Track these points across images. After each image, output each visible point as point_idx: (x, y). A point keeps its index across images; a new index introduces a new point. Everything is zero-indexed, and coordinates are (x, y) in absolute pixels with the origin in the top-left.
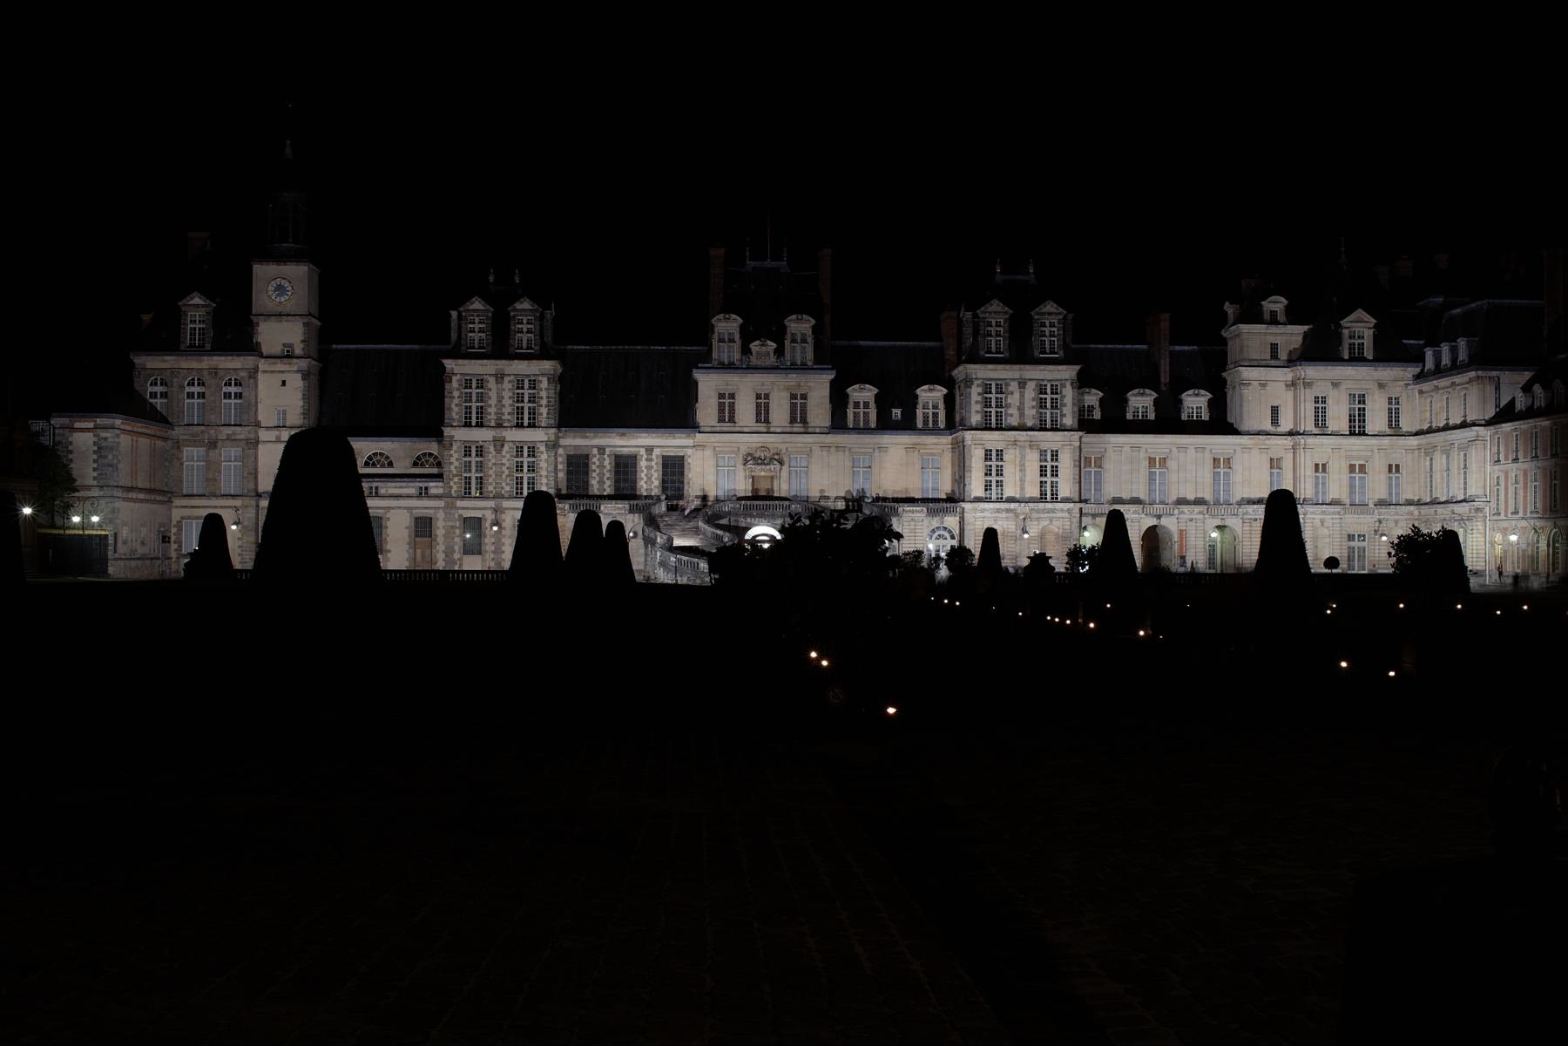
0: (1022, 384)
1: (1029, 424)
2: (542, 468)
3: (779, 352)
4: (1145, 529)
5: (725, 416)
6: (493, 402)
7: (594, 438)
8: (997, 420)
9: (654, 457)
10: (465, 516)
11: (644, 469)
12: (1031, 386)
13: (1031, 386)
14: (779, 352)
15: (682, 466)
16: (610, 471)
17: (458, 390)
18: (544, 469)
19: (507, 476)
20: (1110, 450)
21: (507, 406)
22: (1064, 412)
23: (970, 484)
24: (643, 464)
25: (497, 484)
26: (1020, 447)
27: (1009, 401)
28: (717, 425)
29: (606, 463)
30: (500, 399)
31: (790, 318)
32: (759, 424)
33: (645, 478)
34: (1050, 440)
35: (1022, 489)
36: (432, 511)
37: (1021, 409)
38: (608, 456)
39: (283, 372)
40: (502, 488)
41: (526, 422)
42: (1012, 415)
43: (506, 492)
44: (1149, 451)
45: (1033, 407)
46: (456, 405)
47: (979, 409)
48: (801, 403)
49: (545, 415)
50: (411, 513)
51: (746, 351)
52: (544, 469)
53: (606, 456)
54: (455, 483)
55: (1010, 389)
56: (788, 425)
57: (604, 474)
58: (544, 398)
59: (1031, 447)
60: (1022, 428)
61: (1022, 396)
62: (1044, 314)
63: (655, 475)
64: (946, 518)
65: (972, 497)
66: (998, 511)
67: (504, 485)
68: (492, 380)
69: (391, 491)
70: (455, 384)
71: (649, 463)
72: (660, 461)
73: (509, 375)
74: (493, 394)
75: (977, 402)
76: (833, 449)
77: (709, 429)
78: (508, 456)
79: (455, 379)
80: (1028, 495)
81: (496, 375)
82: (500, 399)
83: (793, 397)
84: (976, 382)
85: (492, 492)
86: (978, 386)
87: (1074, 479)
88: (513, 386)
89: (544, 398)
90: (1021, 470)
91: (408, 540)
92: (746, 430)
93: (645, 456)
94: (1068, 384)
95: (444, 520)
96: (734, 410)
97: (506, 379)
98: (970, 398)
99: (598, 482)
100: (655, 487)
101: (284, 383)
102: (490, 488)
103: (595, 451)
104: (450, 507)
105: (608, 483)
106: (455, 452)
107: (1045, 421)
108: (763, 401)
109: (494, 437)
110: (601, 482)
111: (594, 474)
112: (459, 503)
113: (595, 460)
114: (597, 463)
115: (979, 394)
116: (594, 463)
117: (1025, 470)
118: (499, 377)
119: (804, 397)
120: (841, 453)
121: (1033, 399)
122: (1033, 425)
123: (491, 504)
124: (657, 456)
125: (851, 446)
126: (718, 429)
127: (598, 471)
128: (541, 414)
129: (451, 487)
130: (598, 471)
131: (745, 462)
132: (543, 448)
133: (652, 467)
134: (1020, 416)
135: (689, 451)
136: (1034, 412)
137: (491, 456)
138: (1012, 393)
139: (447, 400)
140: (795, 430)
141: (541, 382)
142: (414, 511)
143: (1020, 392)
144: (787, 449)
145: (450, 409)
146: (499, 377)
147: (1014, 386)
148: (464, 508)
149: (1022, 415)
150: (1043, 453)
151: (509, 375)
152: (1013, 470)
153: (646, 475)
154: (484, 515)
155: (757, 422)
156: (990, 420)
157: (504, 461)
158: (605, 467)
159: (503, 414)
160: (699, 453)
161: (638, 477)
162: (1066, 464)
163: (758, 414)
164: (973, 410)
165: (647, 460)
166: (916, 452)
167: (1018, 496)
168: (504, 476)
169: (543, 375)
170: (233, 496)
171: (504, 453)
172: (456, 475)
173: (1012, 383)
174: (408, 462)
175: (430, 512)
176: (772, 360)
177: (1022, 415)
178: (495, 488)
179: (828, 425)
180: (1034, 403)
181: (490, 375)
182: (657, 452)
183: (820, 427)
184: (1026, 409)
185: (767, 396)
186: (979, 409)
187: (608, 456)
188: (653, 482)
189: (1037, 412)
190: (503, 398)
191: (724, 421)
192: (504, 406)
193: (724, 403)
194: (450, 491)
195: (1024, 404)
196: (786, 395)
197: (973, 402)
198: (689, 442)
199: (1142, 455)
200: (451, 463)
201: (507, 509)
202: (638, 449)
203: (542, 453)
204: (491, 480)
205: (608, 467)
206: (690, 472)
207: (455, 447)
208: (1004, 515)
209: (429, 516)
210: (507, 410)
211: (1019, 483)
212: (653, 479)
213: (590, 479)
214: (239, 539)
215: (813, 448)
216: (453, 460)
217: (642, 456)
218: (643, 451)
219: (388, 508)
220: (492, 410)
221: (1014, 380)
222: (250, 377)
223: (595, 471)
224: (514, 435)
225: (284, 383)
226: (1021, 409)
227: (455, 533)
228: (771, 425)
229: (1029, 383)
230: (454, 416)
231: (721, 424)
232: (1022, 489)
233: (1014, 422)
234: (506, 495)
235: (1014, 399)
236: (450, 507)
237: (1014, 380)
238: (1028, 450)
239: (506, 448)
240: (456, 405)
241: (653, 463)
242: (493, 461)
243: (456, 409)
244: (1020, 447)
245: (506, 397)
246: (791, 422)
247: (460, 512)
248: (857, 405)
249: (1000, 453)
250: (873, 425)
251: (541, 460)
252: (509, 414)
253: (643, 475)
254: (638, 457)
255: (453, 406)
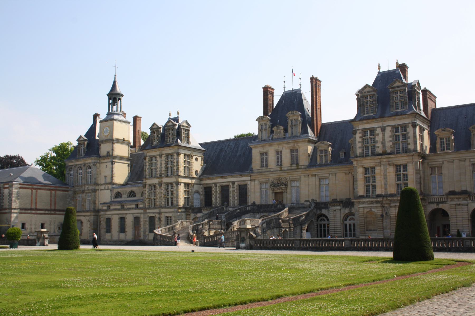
0: (383, 129)
1: (389, 151)
2: (174, 194)
3: (286, 131)
4: (472, 210)
5: (264, 164)
6: (159, 166)
7: (213, 179)
8: (372, 151)
9: (235, 186)
10: (150, 216)
11: (231, 192)
12: (388, 130)
13: (388, 130)
14: (286, 131)
15: (246, 189)
16: (219, 194)
17: (148, 162)
18: (175, 194)
19: (163, 198)
20: (445, 163)
21: (163, 167)
22: (409, 142)
23: (357, 188)
24: (231, 189)
25: (160, 201)
26: (383, 165)
27: (377, 139)
28: (260, 169)
29: (218, 190)
30: (161, 164)
31: (289, 113)
32: (277, 167)
33: (232, 196)
34: (401, 159)
35: (386, 189)
36: (139, 215)
37: (383, 143)
38: (218, 187)
39: (106, 162)
40: (161, 203)
41: (170, 174)
42: (378, 147)
43: (163, 205)
44: (472, 160)
45: (390, 141)
46: (148, 169)
47: (361, 146)
48: (296, 154)
49: (176, 170)
50: (133, 216)
51: (272, 132)
52: (175, 194)
53: (217, 187)
54: (147, 202)
55: (377, 132)
56: (290, 166)
57: (217, 195)
58: (176, 162)
59: (389, 164)
60: (384, 153)
61: (384, 135)
62: (394, 88)
63: (236, 194)
64: (352, 209)
65: (358, 195)
66: (372, 202)
67: (162, 202)
68: (158, 157)
69: (128, 207)
70: (147, 160)
71: (233, 189)
72: (238, 187)
73: (164, 154)
74: (159, 163)
75: (359, 142)
76: (310, 176)
77: (256, 171)
78: (163, 189)
79: (147, 158)
80: (389, 193)
81: (159, 155)
82: (161, 164)
83: (292, 151)
84: (358, 132)
85: (158, 205)
86: (360, 133)
87: (416, 181)
88: (165, 158)
89: (176, 162)
90: (384, 178)
91: (132, 227)
92: (272, 170)
93: (232, 186)
94: (410, 125)
95: (143, 218)
96: (267, 161)
97: (163, 156)
98: (356, 140)
99: (215, 199)
100: (236, 200)
101: (107, 165)
102: (158, 203)
103: (213, 185)
104: (145, 213)
105: (218, 199)
106: (147, 189)
107: (399, 148)
108: (279, 155)
109: (159, 181)
110: (216, 199)
111: (213, 196)
112: (148, 211)
113: (213, 189)
114: (214, 191)
115: (360, 137)
116: (213, 191)
117: (387, 178)
118: (161, 156)
119: (297, 150)
120: (314, 178)
121: (390, 137)
122: (391, 151)
123: (157, 211)
124: (236, 186)
125: (319, 173)
126: (260, 170)
127: (214, 194)
128: (174, 170)
129: (145, 204)
130: (214, 194)
131: (271, 185)
132: (174, 185)
133: (234, 191)
134: (383, 147)
135: (249, 182)
136: (391, 144)
137: (158, 190)
138: (378, 135)
139: (145, 167)
140: (293, 168)
141: (174, 156)
142: (134, 215)
143: (382, 133)
144: (289, 178)
145: (145, 171)
146: (161, 156)
147: (379, 131)
148: (149, 213)
149: (384, 146)
150: (398, 167)
151: (164, 154)
152: (380, 179)
153: (232, 195)
154: (155, 215)
155: (277, 165)
156: (368, 151)
157: (162, 191)
158: (217, 192)
159: (162, 171)
160: (253, 183)
161: (229, 195)
162: (411, 170)
163: (278, 162)
164: (357, 147)
165: (232, 188)
166: (350, 174)
167: (383, 194)
168: (162, 198)
169: (175, 153)
170: (87, 211)
171: (162, 188)
172: (147, 199)
173: (378, 129)
174: (140, 195)
175: (138, 215)
176: (282, 135)
177: (384, 146)
178: (159, 203)
179: (307, 164)
180: (391, 139)
181: (158, 155)
182: (236, 184)
183: (303, 165)
184: (386, 143)
185: (281, 152)
186: (361, 146)
187: (218, 187)
188: (235, 198)
189: (393, 144)
190: (162, 164)
191: (264, 167)
192: (162, 167)
193: (264, 158)
194: (145, 206)
195: (385, 140)
196: (288, 151)
197: (357, 142)
198: (248, 178)
199: (467, 163)
200: (146, 194)
201: (162, 212)
202: (229, 183)
203: (174, 187)
204: (158, 200)
205: (218, 192)
206: (249, 192)
207: (147, 187)
208: (375, 205)
209: (138, 216)
210: (163, 169)
211: (384, 186)
212: (235, 197)
213: (212, 198)
214: (89, 228)
215: (301, 176)
216: (146, 192)
217: (231, 186)
218: (231, 184)
219: (126, 214)
220: (158, 170)
221: (378, 127)
222: (94, 165)
223: (213, 194)
224: (165, 180)
225: (107, 165)
226: (383, 143)
227: (146, 223)
228: (283, 166)
229: (387, 128)
230: (147, 174)
231: (262, 168)
232: (386, 189)
233: (379, 150)
234: (163, 206)
235: (379, 138)
236: (145, 213)
237: (378, 127)
238: (388, 167)
239: (163, 186)
240: (148, 169)
241: (235, 189)
242: (159, 191)
243: (147, 171)
244: (383, 165)
245: (163, 164)
246: (291, 165)
247: (148, 214)
248: (321, 151)
249: (373, 169)
250: (329, 162)
251: (174, 190)
252: (164, 171)
253: (231, 195)
254: (229, 187)
255: (146, 169)
